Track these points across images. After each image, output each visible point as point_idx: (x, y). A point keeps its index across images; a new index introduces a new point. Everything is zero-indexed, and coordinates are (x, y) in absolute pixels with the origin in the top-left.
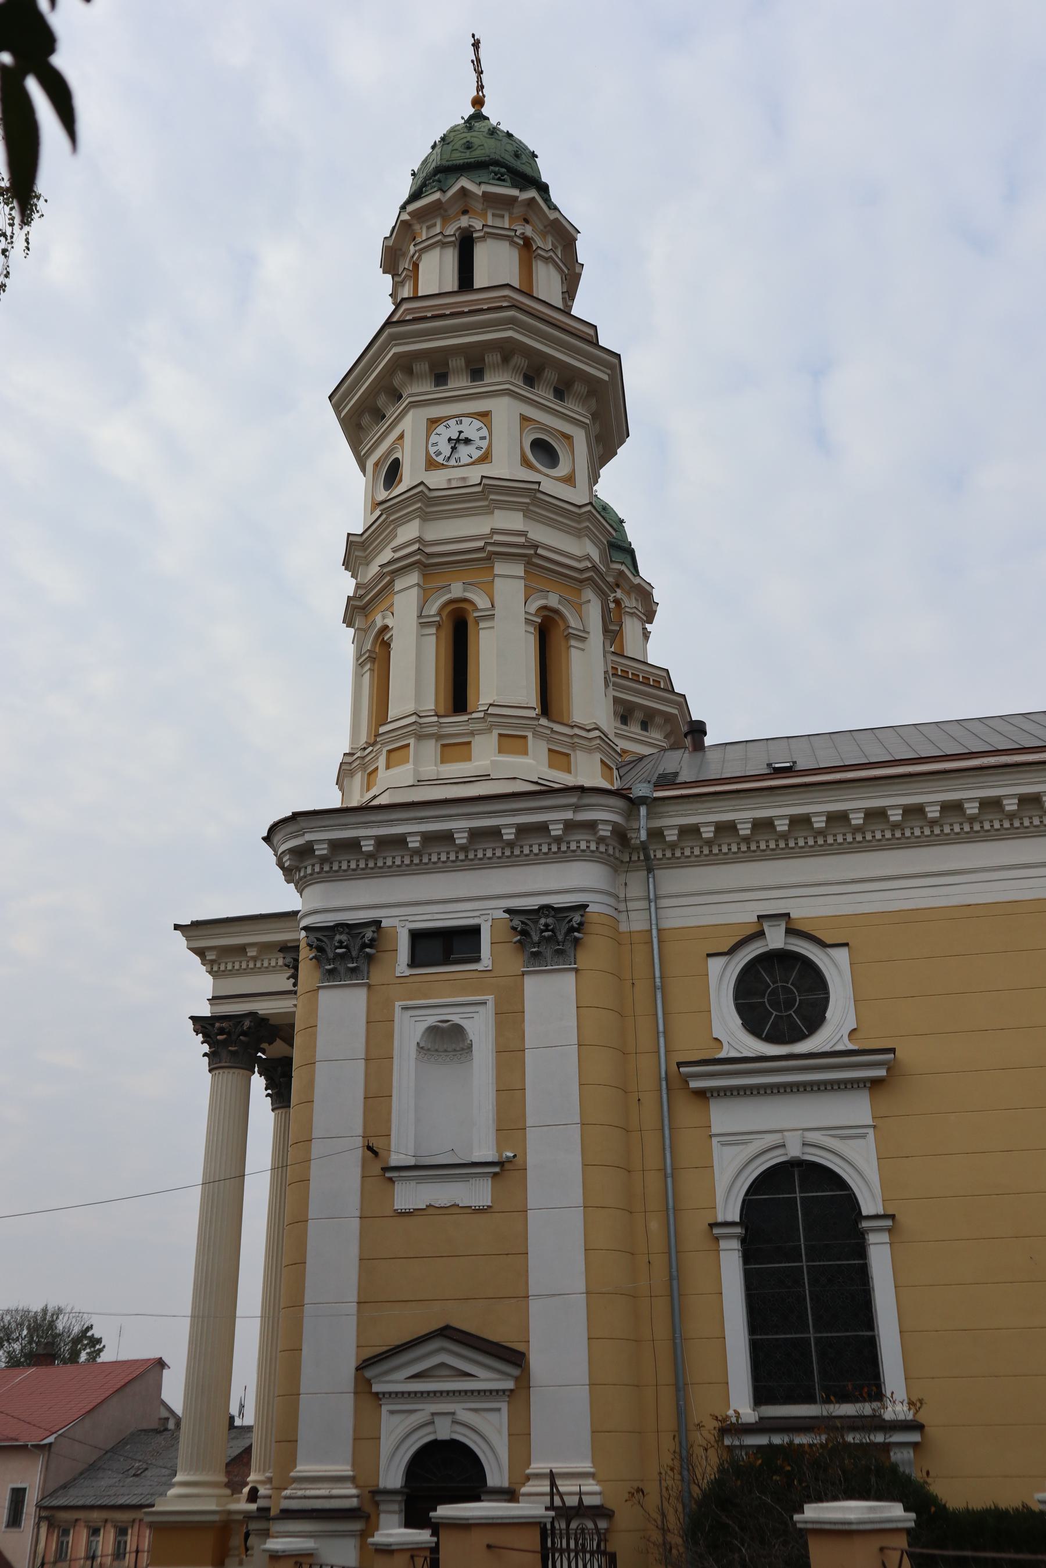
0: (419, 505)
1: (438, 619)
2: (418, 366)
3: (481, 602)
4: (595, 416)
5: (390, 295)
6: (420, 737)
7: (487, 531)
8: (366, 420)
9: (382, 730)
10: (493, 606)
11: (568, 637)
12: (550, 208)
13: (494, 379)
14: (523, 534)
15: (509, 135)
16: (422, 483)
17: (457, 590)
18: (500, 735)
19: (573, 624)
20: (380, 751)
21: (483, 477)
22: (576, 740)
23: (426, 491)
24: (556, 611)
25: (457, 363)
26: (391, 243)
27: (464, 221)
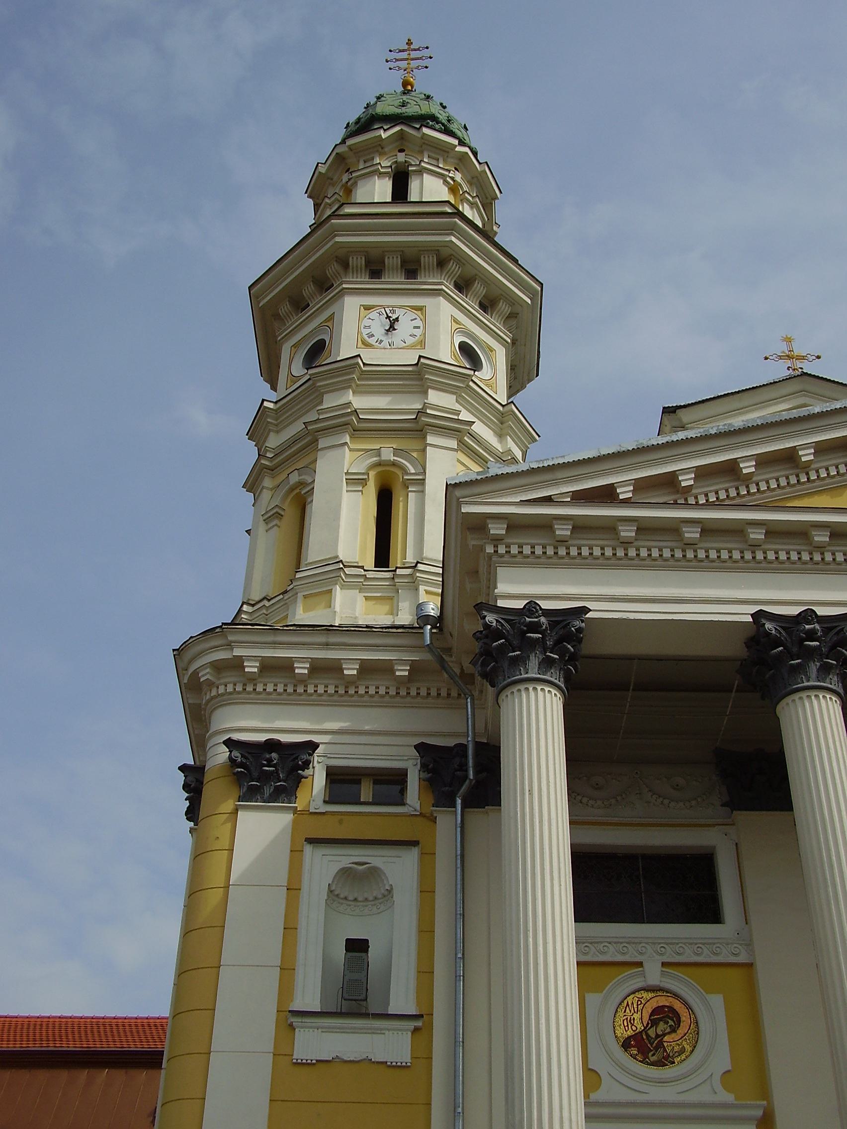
11: (406, 485)
17: (294, 478)
18: (305, 597)
24: (394, 464)
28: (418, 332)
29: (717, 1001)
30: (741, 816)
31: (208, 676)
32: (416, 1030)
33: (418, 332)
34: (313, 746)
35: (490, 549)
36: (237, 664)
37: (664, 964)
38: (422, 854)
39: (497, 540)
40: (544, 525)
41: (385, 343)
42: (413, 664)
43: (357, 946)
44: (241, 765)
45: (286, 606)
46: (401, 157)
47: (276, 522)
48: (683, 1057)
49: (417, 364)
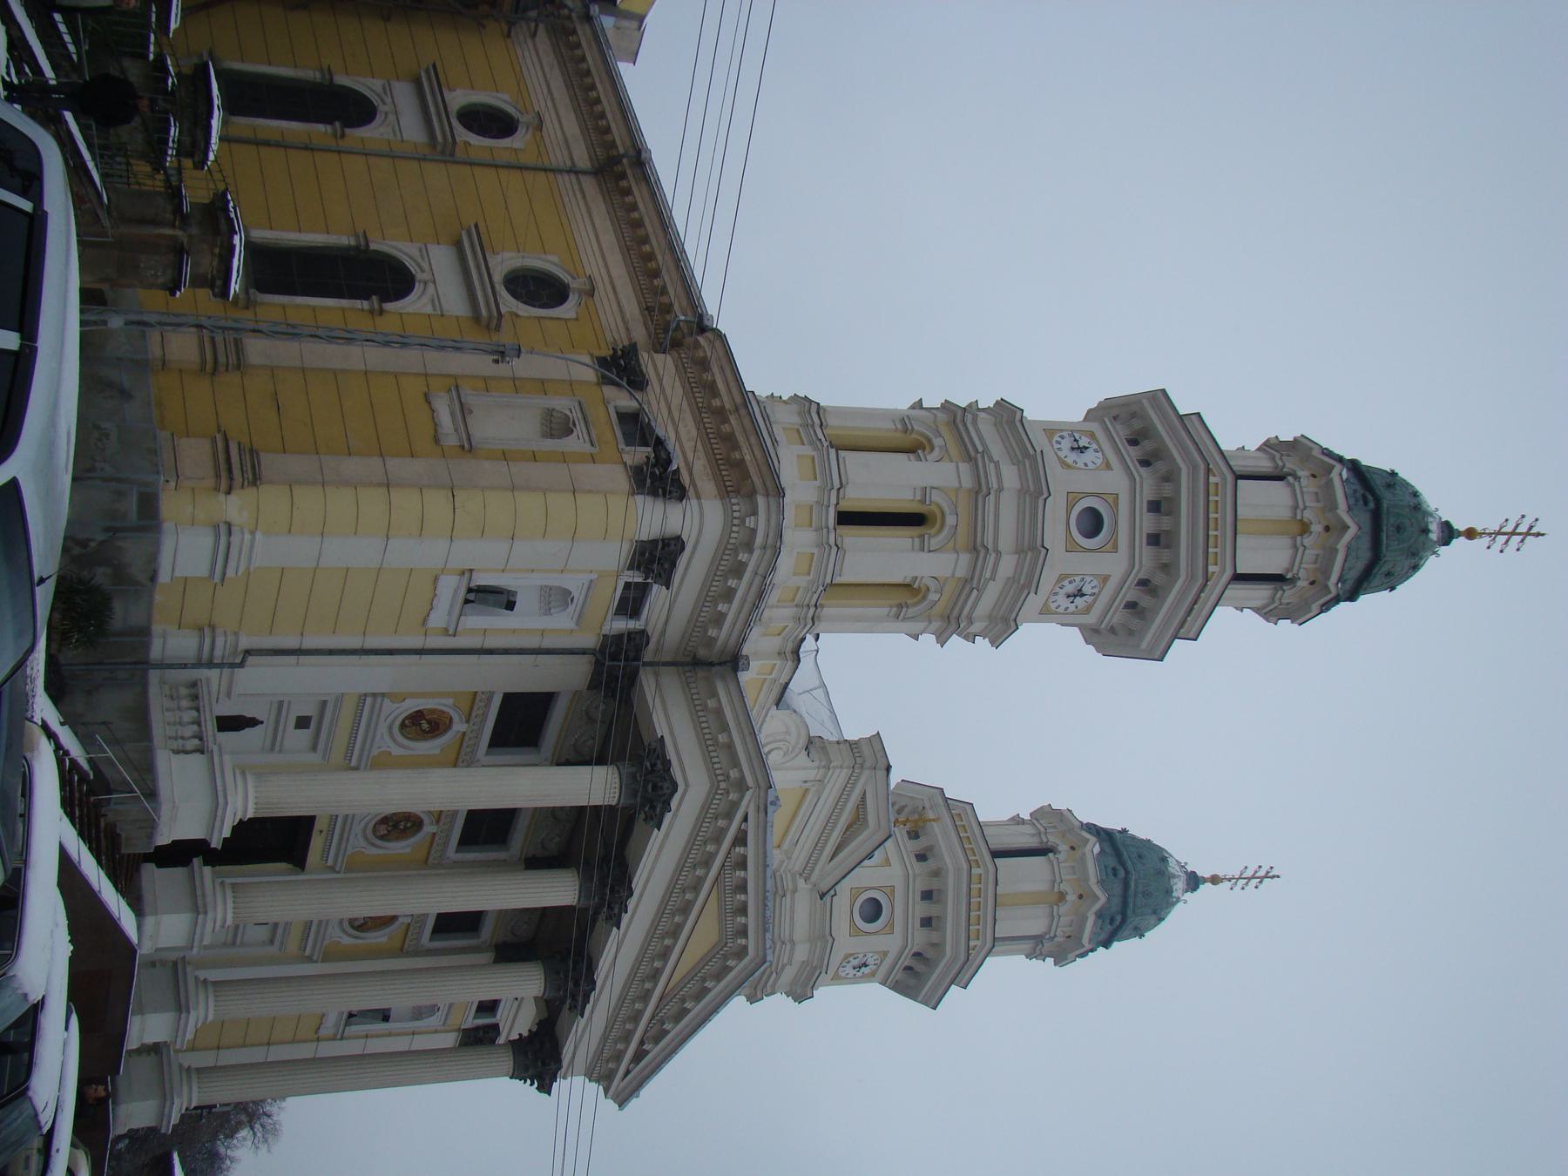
0: (1032, 489)
1: (927, 503)
2: (1167, 488)
3: (935, 542)
4: (1112, 630)
5: (1277, 437)
9: (832, 452)
10: (930, 551)
11: (900, 606)
12: (1322, 606)
13: (1146, 555)
14: (993, 578)
15: (1415, 568)
17: (951, 520)
18: (813, 554)
19: (910, 610)
20: (816, 449)
21: (1047, 550)
22: (805, 609)
23: (1045, 496)
24: (924, 598)
25: (1165, 523)
26: (1316, 453)
29: (437, 751)
31: (747, 524)
32: (446, 630)
34: (668, 589)
36: (749, 546)
39: (728, 793)
40: (729, 816)
41: (1057, 589)
43: (510, 606)
44: (663, 548)
45: (819, 529)
47: (918, 498)
48: (407, 735)
49: (1015, 620)
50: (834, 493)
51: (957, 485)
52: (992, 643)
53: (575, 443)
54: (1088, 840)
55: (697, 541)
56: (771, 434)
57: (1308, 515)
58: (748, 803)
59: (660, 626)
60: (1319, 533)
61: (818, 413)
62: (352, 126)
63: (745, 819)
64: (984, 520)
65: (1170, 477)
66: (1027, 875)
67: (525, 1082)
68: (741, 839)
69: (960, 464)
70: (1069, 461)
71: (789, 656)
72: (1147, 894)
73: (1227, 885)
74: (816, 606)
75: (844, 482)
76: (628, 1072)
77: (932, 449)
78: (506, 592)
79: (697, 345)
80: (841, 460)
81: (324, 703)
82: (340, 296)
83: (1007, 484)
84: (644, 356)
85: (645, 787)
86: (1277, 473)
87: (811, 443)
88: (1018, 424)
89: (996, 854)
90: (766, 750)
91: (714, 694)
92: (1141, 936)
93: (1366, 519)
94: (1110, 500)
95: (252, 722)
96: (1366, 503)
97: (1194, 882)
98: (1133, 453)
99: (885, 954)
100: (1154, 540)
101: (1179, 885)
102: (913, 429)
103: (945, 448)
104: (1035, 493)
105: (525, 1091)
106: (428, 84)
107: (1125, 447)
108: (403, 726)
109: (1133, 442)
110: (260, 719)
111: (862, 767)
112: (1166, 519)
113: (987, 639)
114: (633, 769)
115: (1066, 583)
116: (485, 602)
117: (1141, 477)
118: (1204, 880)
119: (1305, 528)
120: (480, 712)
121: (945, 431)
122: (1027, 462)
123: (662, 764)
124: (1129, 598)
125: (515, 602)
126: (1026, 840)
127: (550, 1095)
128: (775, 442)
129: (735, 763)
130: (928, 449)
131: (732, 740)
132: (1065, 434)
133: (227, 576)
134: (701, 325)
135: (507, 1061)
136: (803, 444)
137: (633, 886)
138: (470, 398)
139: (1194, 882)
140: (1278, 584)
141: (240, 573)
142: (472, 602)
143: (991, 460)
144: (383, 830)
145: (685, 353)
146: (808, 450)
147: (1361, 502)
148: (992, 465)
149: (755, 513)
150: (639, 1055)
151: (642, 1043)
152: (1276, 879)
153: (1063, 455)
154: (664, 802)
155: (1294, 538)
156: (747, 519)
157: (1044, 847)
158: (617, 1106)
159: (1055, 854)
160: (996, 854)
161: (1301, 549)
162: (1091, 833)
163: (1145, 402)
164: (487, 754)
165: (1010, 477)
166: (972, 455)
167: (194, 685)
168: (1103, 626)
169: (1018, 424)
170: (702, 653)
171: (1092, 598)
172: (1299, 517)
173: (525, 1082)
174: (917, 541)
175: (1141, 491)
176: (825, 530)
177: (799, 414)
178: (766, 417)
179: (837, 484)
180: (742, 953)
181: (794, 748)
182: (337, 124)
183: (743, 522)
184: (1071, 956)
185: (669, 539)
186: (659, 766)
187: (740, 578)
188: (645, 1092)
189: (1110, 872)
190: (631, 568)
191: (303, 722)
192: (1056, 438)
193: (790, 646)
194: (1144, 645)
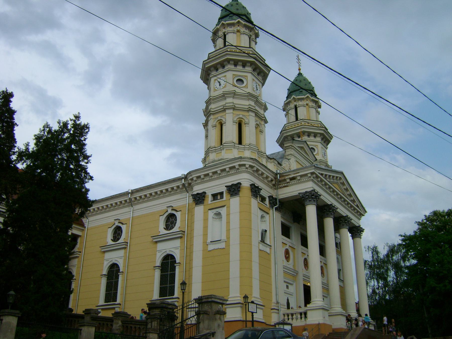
0: (233, 95)
3: (247, 121)
6: (234, 148)
7: (248, 104)
8: (212, 69)
9: (224, 145)
10: (249, 122)
11: (261, 131)
14: (255, 107)
16: (235, 91)
17: (241, 116)
18: (251, 152)
20: (223, 149)
24: (258, 125)
27: (238, 28)
28: (259, 92)
30: (295, 223)
33: (259, 92)
34: (262, 189)
35: (312, 178)
37: (289, 246)
38: (269, 216)
41: (256, 92)
42: (271, 179)
45: (244, 149)
46: (251, 33)
47: (235, 124)
49: (263, 103)
50: (236, 145)
51: (232, 114)
52: (267, 110)
53: (223, 211)
54: (294, 98)
55: (251, 180)
56: (219, 160)
57: (235, 30)
58: (317, 172)
59: (268, 193)
60: (240, 28)
61: (212, 148)
62: (119, 269)
63: (319, 173)
64: (241, 108)
65: (228, 61)
66: (302, 113)
67: (362, 235)
68: (322, 174)
69: (226, 113)
70: (224, 86)
71: (272, 161)
72: (306, 84)
73: (300, 66)
74: (261, 152)
75: (232, 142)
76: (360, 209)
77: (221, 120)
78: (262, 232)
79: (192, 179)
80: (226, 143)
81: (285, 282)
82: (175, 274)
83: (231, 101)
84: (195, 193)
85: (313, 198)
86: (223, 37)
87: (221, 150)
88: (214, 98)
89: (297, 119)
90: (289, 170)
91: (285, 180)
92: (314, 88)
93: (235, 17)
94: (234, 76)
95: (288, 300)
96: (232, 16)
97: (300, 74)
98: (221, 70)
99: (322, 148)
100: (244, 66)
101: (301, 78)
102: (215, 124)
103: (221, 117)
104: (234, 95)
105: (364, 235)
106: (105, 250)
107: (218, 72)
108: (288, 261)
109: (217, 70)
110: (287, 298)
111: (292, 146)
112: (239, 63)
113: (266, 111)
114: (308, 201)
115: (254, 89)
116: (264, 238)
117: (228, 68)
118: (300, 72)
119: (238, 31)
120: (285, 241)
121: (216, 116)
122: (225, 96)
123: (306, 193)
124: (257, 74)
125: (265, 230)
126: (293, 112)
127: (364, 229)
128: (221, 159)
129: (306, 175)
130: (221, 121)
131: (299, 175)
132: (215, 87)
133: (262, 305)
134: (185, 177)
135: (357, 239)
136: (221, 152)
137: (329, 204)
138: (209, 240)
139: (300, 74)
140: (251, 40)
141: (261, 301)
142: (264, 241)
143: (225, 105)
144: (306, 268)
145: (194, 182)
146: (223, 152)
147: (232, 17)
148: (226, 105)
149: (244, 165)
150: (357, 206)
151: (355, 205)
152: (299, 56)
153: (221, 88)
154: (316, 193)
155: (241, 34)
156: (247, 167)
157: (294, 108)
158: (366, 213)
159: (297, 106)
160: (297, 119)
161: (244, 32)
162: (291, 97)
163: (206, 66)
164: (292, 240)
165: (229, 100)
166: (224, 110)
167: (284, 315)
168: (262, 82)
169: (214, 98)
170: (274, 182)
171: (257, 84)
172: (236, 32)
173: (362, 235)
174: (246, 125)
175: (233, 68)
176: (245, 148)
177: (212, 153)
178: (213, 162)
179: (233, 144)
180: (340, 178)
181: (289, 163)
182: (119, 274)
183: (247, 168)
184: (320, 104)
185: (251, 188)
186: (307, 194)
187: (259, 170)
188: (364, 206)
189: (301, 93)
190: (257, 198)
191: (287, 287)
192: (216, 89)
193: (269, 160)
194: (268, 73)
